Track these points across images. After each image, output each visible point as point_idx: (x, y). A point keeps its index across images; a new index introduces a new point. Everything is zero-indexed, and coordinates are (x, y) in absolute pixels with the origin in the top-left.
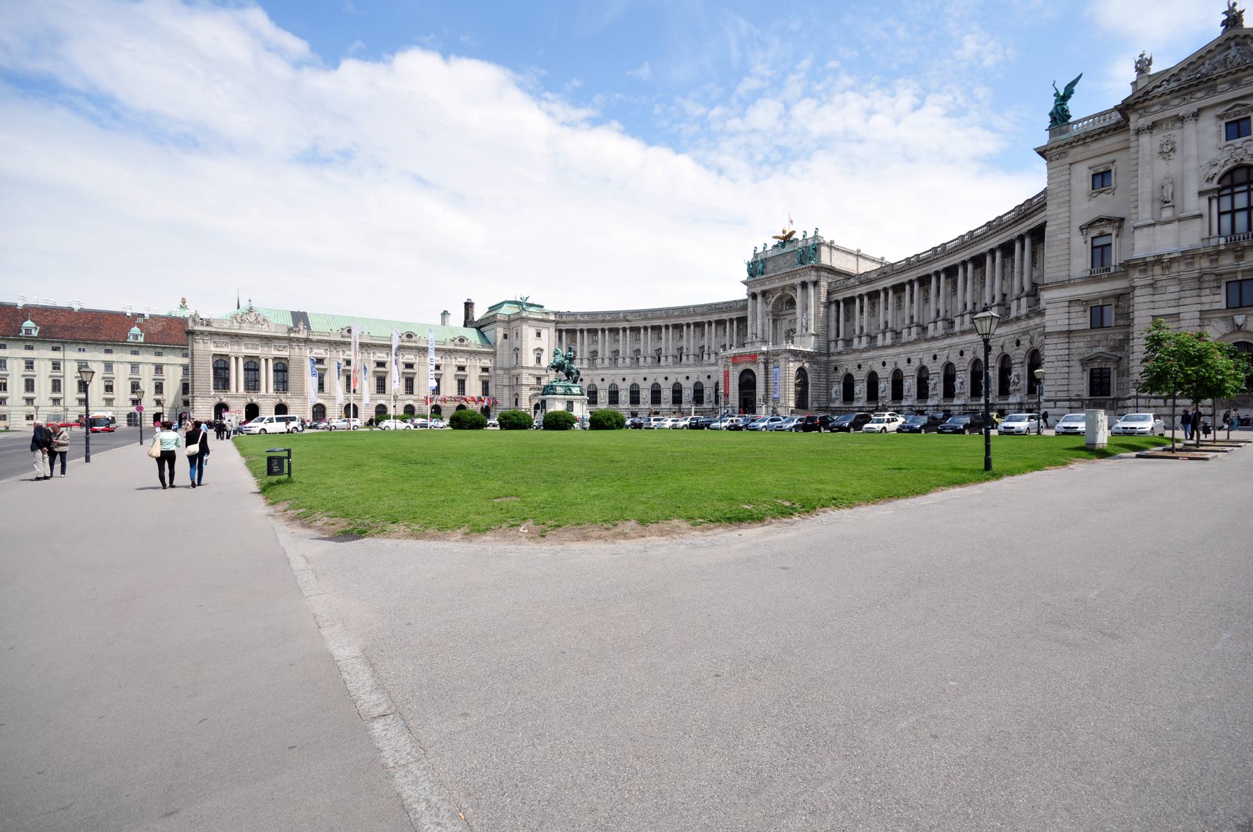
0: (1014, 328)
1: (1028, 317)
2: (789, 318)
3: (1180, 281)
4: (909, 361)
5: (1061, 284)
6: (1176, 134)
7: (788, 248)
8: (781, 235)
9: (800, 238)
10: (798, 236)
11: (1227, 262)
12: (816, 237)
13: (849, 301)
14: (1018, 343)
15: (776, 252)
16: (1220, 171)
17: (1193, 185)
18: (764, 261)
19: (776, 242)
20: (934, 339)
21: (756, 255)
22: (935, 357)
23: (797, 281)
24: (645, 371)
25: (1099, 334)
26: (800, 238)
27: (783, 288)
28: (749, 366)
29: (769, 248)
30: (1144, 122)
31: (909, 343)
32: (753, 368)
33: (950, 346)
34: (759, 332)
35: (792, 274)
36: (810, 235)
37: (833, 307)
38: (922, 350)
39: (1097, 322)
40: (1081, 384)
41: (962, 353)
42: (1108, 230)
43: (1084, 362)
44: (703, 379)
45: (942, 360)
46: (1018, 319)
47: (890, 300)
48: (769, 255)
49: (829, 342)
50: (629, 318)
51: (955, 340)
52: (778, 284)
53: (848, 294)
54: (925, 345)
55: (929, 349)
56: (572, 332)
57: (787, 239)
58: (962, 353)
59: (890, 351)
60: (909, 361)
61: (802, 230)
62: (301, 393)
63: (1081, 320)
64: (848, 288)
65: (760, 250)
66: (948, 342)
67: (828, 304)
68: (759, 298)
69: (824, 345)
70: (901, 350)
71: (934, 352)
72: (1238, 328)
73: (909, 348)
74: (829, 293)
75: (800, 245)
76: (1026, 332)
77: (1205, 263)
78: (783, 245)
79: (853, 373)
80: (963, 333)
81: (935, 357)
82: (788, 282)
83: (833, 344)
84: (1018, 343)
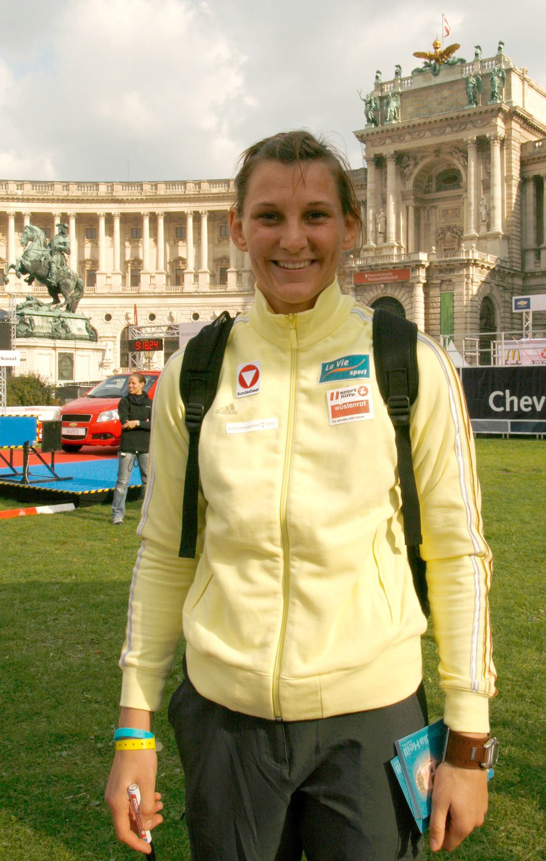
2: (442, 205)
8: (432, 51)
9: (470, 59)
10: (465, 53)
15: (420, 83)
19: (420, 63)
21: (379, 86)
23: (471, 136)
27: (438, 151)
28: (390, 293)
29: (406, 73)
35: (460, 122)
36: (489, 52)
37: (531, 189)
49: (524, 252)
50: (119, 192)
52: (429, 140)
65: (388, 76)
67: (524, 181)
68: (391, 167)
69: (516, 257)
74: (523, 163)
83: (531, 257)
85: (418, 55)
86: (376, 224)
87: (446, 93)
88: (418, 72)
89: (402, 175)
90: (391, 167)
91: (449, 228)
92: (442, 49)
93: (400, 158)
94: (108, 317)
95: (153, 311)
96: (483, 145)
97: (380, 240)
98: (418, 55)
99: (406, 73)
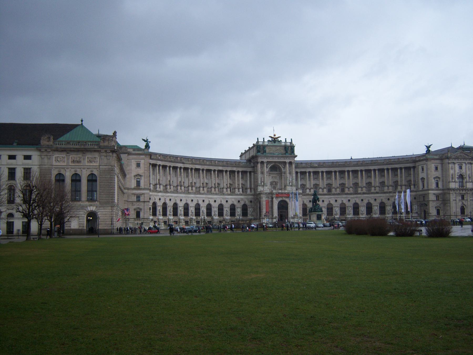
0: (387, 195)
2: (272, 175)
3: (456, 193)
4: (336, 201)
5: (432, 190)
7: (277, 144)
8: (273, 136)
9: (283, 141)
11: (461, 192)
12: (291, 143)
13: (303, 173)
14: (389, 199)
15: (270, 144)
16: (459, 174)
18: (264, 147)
19: (270, 139)
20: (347, 194)
21: (258, 142)
22: (349, 200)
24: (193, 196)
25: (438, 202)
26: (284, 141)
28: (284, 199)
32: (287, 200)
33: (357, 197)
34: (266, 182)
36: (289, 141)
39: (438, 199)
41: (362, 200)
42: (438, 179)
43: (435, 207)
44: (224, 202)
45: (353, 201)
46: (390, 192)
48: (266, 143)
53: (303, 170)
55: (346, 197)
56: (154, 166)
57: (275, 140)
58: (362, 200)
59: (326, 196)
60: (336, 201)
61: (284, 137)
62: (110, 203)
63: (435, 198)
64: (303, 168)
65: (261, 140)
66: (355, 196)
68: (265, 165)
71: (349, 199)
72: (463, 203)
75: (283, 144)
77: (458, 191)
79: (307, 204)
80: (364, 193)
81: (349, 200)
82: (282, 160)
84: (389, 199)
85: (270, 137)
86: (261, 179)
87: (278, 148)
88: (269, 141)
90: (265, 165)
91: (274, 182)
92: (277, 136)
93: (268, 163)
94: (181, 200)
95: (192, 198)
97: (262, 184)
98: (270, 137)
99: (266, 140)
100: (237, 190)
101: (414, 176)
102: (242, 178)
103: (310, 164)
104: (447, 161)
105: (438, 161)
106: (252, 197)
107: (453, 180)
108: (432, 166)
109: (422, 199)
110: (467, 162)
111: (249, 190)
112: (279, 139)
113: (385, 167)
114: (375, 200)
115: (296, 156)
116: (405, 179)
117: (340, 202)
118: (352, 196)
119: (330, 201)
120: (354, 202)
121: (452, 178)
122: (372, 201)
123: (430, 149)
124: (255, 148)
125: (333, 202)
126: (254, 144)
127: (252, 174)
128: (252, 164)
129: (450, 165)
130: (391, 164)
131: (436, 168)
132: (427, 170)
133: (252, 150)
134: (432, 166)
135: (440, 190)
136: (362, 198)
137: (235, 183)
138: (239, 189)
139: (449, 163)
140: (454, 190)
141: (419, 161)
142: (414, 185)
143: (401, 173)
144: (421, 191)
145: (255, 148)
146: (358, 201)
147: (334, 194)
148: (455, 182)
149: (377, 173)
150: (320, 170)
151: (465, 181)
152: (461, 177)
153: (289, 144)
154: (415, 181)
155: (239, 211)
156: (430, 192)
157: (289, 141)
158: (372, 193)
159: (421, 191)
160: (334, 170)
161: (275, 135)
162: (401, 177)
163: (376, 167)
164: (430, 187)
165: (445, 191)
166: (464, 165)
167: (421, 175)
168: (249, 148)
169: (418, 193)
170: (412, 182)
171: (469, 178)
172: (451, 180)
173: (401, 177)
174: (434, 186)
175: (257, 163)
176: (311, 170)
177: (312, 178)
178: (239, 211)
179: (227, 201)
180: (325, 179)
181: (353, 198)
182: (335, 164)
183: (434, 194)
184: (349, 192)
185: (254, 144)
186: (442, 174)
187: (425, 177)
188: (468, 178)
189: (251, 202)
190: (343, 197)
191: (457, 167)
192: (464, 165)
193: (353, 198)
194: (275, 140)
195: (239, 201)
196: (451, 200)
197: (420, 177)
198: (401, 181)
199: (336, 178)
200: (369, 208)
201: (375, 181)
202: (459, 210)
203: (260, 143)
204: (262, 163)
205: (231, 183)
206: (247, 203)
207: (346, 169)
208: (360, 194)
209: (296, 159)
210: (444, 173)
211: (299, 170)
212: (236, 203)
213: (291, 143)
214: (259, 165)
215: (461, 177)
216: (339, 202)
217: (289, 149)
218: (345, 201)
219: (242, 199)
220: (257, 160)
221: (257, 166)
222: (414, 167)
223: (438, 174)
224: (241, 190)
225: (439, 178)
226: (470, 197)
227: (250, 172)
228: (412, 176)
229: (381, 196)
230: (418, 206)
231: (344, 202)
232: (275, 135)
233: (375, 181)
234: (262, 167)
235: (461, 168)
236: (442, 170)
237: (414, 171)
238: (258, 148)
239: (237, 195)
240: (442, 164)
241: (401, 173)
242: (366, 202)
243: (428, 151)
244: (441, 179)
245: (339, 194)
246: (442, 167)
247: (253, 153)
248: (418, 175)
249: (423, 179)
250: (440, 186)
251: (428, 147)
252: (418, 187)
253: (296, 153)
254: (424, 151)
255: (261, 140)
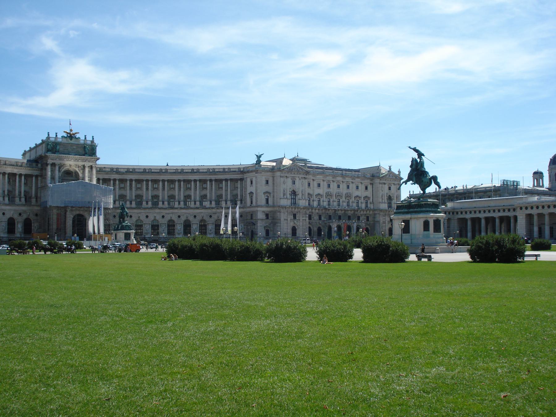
0: (209, 211)
1: (218, 209)
4: (147, 217)
5: (261, 206)
6: (286, 179)
7: (73, 141)
8: (68, 131)
9: (82, 138)
14: (211, 216)
15: (65, 141)
17: (288, 193)
19: (65, 135)
21: (48, 138)
22: (163, 217)
23: (87, 164)
26: (82, 138)
28: (81, 213)
30: (282, 175)
31: (148, 208)
33: (173, 213)
36: (89, 138)
38: (155, 213)
40: (264, 234)
41: (179, 217)
45: (168, 218)
46: (213, 208)
47: (134, 186)
48: (60, 140)
51: (176, 211)
53: (106, 177)
54: (157, 211)
55: (160, 213)
57: (71, 136)
58: (179, 217)
60: (147, 217)
63: (264, 217)
65: (52, 135)
66: (171, 211)
68: (57, 168)
70: (143, 211)
71: (163, 214)
73: (147, 211)
75: (82, 142)
76: (215, 213)
78: (71, 140)
80: (181, 208)
81: (163, 217)
84: (211, 216)
89: (59, 171)
90: (57, 168)
92: (74, 132)
96: (91, 167)
99: (59, 136)
100: (17, 200)
101: (242, 190)
102: (25, 184)
103: (115, 170)
104: (278, 174)
105: (270, 174)
106: (39, 208)
107: (285, 197)
108: (262, 178)
109: (249, 217)
110: (301, 176)
111: (34, 201)
112: (77, 136)
113: (208, 177)
114: (195, 217)
115: (98, 159)
116: (231, 193)
117: (152, 218)
118: (167, 211)
119: (139, 217)
120: (169, 218)
121: (284, 195)
122: (191, 218)
123: (261, 159)
124: (44, 145)
125: (143, 218)
126: (42, 140)
127: (39, 178)
128: (39, 165)
129: (282, 179)
130: (215, 175)
131: (267, 182)
132: (256, 184)
133: (40, 147)
134: (262, 178)
135: (271, 207)
136: (179, 214)
137: (15, 190)
138: (20, 198)
139: (281, 177)
140: (285, 207)
141: (248, 172)
142: (241, 201)
143: (227, 186)
144: (249, 207)
145: (44, 145)
146: (175, 218)
147: (145, 209)
148: (287, 198)
149: (198, 185)
150: (129, 177)
151: (297, 198)
152: (294, 193)
153: (89, 143)
154: (242, 196)
155: (19, 227)
156: (259, 209)
157: (89, 138)
158: (192, 208)
159: (249, 207)
160: (145, 179)
161: (71, 130)
162: (226, 190)
163: (197, 177)
164: (259, 203)
165: (275, 209)
166: (297, 179)
167: (249, 189)
168: (36, 144)
169: (245, 210)
170: (239, 197)
171: (303, 195)
172: (282, 196)
173: (226, 190)
174: (264, 202)
175: (47, 165)
176: (117, 177)
177: (117, 187)
178: (19, 227)
179: (4, 214)
180: (134, 189)
181: (169, 214)
182: (147, 171)
183: (263, 212)
184: (164, 207)
185: (42, 140)
186: (274, 189)
187: (254, 192)
188: (300, 195)
189: (37, 215)
190: (155, 213)
191: (289, 181)
192: (297, 179)
193: (169, 214)
194: (71, 136)
195: (20, 214)
196: (282, 219)
197: (248, 192)
198: (226, 195)
199: (147, 189)
200: (187, 227)
201: (195, 194)
202: (290, 231)
203: (51, 139)
204: (53, 165)
205: (11, 189)
206: (32, 217)
207: (161, 177)
208: (177, 208)
209: (98, 162)
210: (275, 188)
211: (101, 177)
212: (16, 216)
213: (92, 142)
214: (49, 168)
215: (294, 193)
216: (151, 218)
217: (89, 150)
218: (159, 217)
219: (25, 212)
220: (47, 161)
221: (46, 169)
222: (242, 180)
223: (269, 188)
224: (23, 199)
225: (270, 193)
226: (303, 217)
227: (37, 176)
228: (239, 189)
229: (202, 213)
230: (244, 225)
231: (157, 218)
232: (71, 130)
233: (195, 194)
234: (53, 171)
235: (294, 183)
236: (273, 184)
237: (241, 184)
238: (49, 147)
239: (18, 205)
240: (273, 177)
241: (227, 186)
242: (183, 218)
243: (259, 162)
244: (272, 195)
245: (151, 208)
246: (273, 180)
247: (41, 151)
248: (246, 188)
249: (251, 193)
250: (270, 202)
251: (259, 157)
252: (245, 203)
253: (98, 154)
254: (254, 161)
255: (52, 135)
